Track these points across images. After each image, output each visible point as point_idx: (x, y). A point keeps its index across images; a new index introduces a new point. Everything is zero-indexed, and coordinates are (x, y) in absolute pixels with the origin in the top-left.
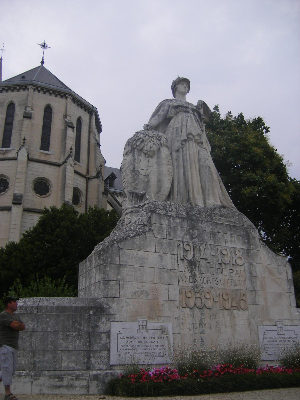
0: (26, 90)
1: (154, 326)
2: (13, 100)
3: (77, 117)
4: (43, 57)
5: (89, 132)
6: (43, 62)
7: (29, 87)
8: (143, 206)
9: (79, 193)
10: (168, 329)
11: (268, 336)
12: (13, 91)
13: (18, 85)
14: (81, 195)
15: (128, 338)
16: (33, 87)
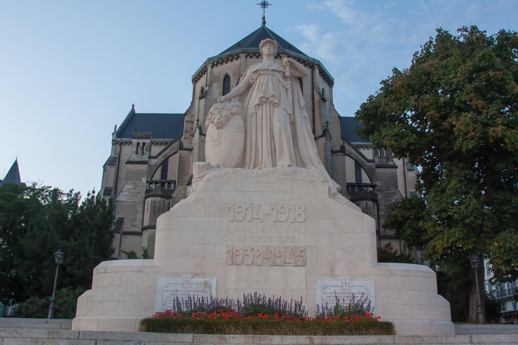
0: (239, 58)
1: (197, 282)
2: (227, 72)
5: (313, 88)
6: (264, 23)
7: (241, 55)
8: (203, 176)
10: (211, 284)
11: (328, 291)
12: (227, 62)
13: (230, 55)
15: (172, 291)
16: (244, 55)
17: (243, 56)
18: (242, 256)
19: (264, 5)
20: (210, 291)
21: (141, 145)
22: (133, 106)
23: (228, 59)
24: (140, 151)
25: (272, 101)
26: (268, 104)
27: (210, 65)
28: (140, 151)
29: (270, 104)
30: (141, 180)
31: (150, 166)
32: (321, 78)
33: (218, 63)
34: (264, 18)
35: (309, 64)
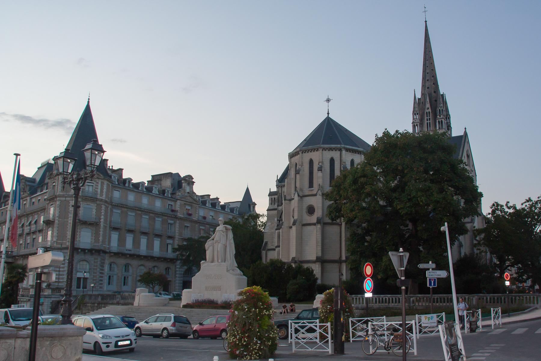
6: (328, 114)
17: (300, 153)
19: (328, 100)
31: (278, 211)
32: (350, 153)
34: (426, 22)
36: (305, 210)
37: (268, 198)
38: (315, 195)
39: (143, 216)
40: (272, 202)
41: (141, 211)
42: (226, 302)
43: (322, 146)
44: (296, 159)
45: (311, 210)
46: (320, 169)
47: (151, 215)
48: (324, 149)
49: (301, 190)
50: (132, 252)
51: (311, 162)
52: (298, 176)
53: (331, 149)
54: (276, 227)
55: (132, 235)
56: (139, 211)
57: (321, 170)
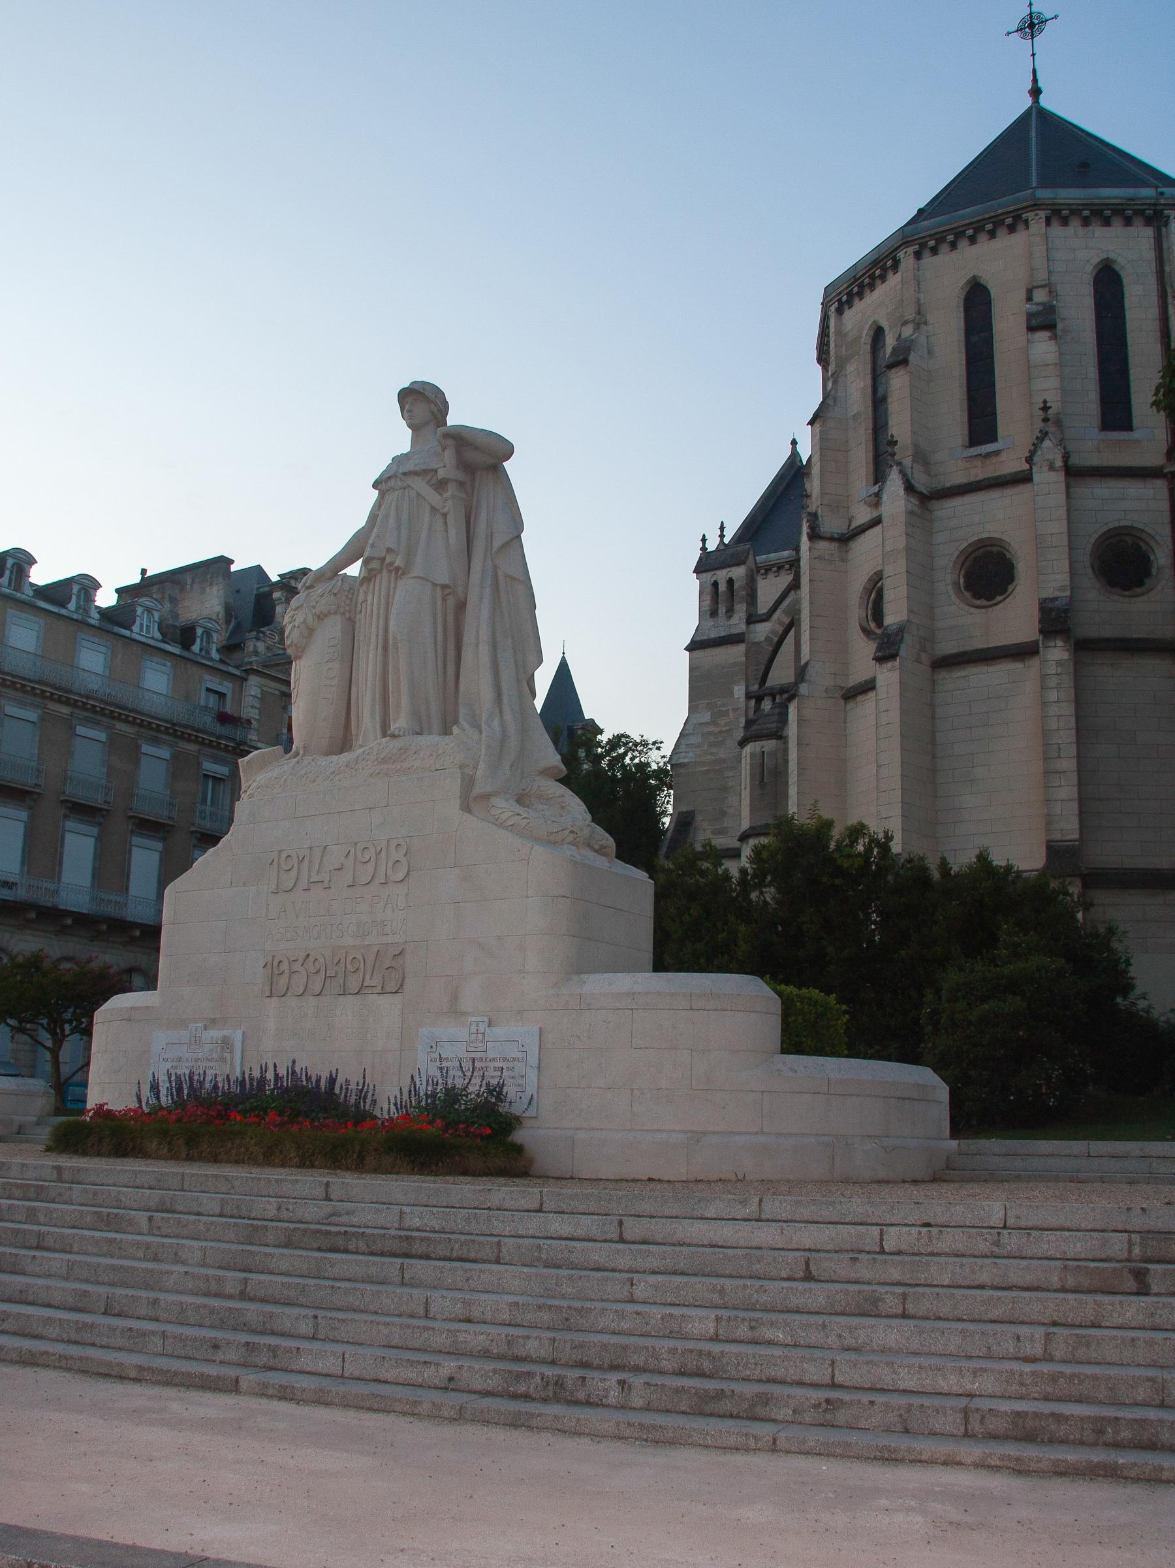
2: (876, 318)
3: (1089, 269)
4: (1034, 71)
6: (1036, 92)
9: (1142, 544)
12: (872, 287)
14: (1152, 543)
16: (911, 250)
17: (906, 257)
18: (287, 972)
19: (1032, 26)
20: (232, 1058)
21: (722, 587)
22: (794, 443)
23: (873, 277)
24: (722, 609)
25: (391, 564)
26: (385, 572)
27: (833, 308)
28: (722, 609)
29: (390, 571)
30: (731, 693)
33: (850, 295)
35: (1139, 213)
36: (947, 577)
37: (692, 586)
38: (1024, 478)
39: (81, 730)
40: (716, 600)
41: (68, 702)
42: (453, 1095)
43: (1044, 194)
44: (875, 306)
45: (988, 572)
46: (1043, 321)
47: (120, 726)
48: (1058, 215)
49: (922, 457)
50: (21, 894)
51: (977, 301)
52: (898, 381)
53: (1099, 215)
54: (739, 734)
55: (24, 815)
56: (59, 701)
57: (1050, 327)
